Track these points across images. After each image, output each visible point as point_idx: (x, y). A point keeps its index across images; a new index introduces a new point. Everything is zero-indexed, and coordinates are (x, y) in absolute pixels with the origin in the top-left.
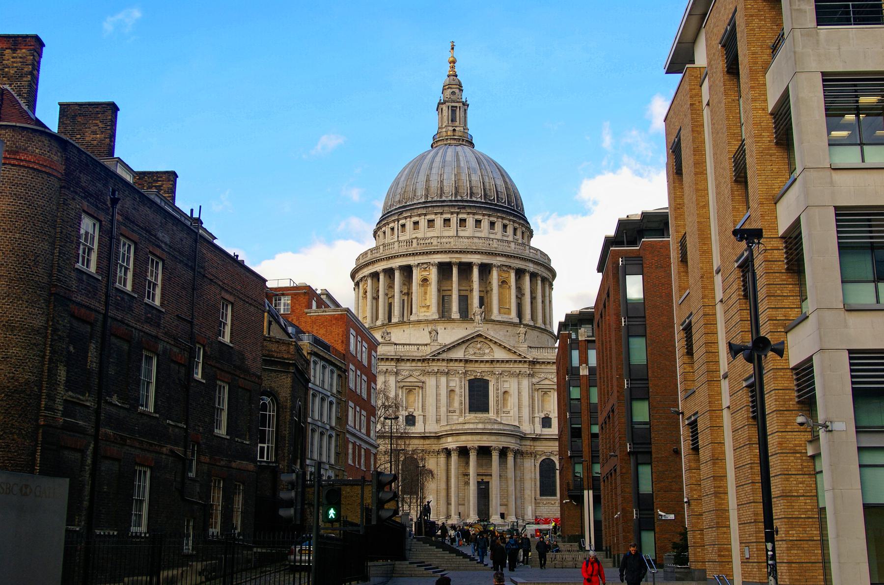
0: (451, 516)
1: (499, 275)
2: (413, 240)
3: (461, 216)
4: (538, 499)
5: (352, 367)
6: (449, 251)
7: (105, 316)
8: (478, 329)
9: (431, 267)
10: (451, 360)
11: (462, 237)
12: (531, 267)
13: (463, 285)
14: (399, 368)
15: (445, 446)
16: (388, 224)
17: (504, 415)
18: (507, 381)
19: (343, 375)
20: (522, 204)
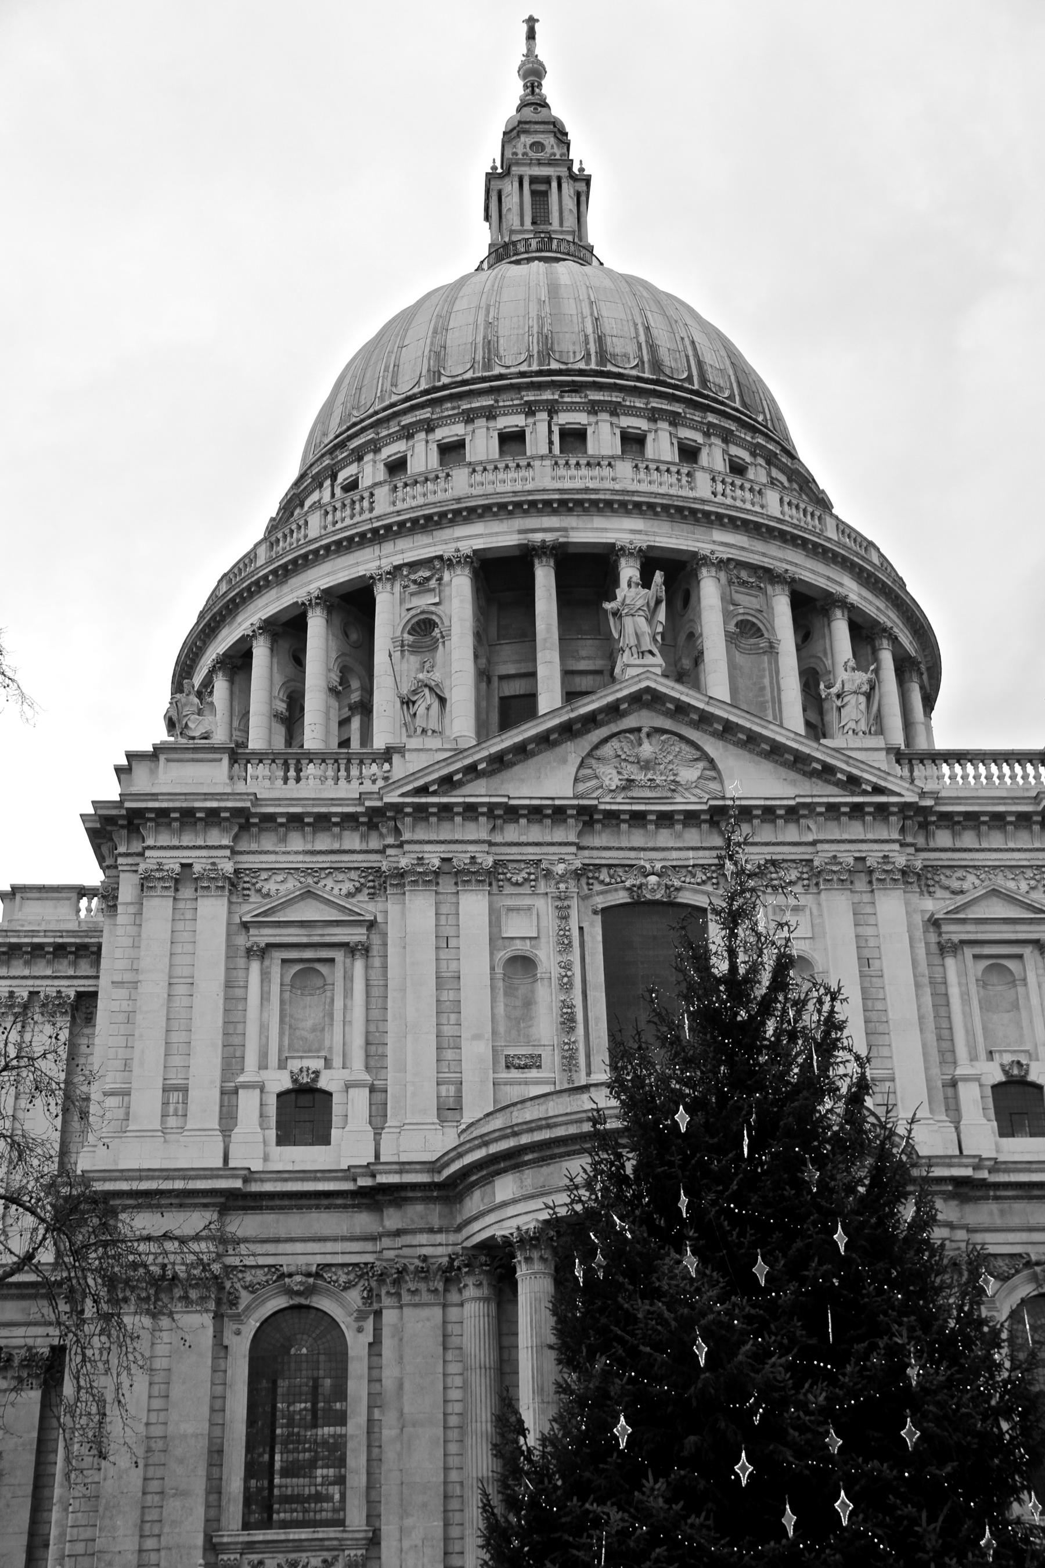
2: (376, 492)
3: (564, 418)
6: (518, 505)
9: (446, 576)
10: (511, 813)
12: (852, 590)
13: (583, 653)
14: (249, 861)
15: (481, 1231)
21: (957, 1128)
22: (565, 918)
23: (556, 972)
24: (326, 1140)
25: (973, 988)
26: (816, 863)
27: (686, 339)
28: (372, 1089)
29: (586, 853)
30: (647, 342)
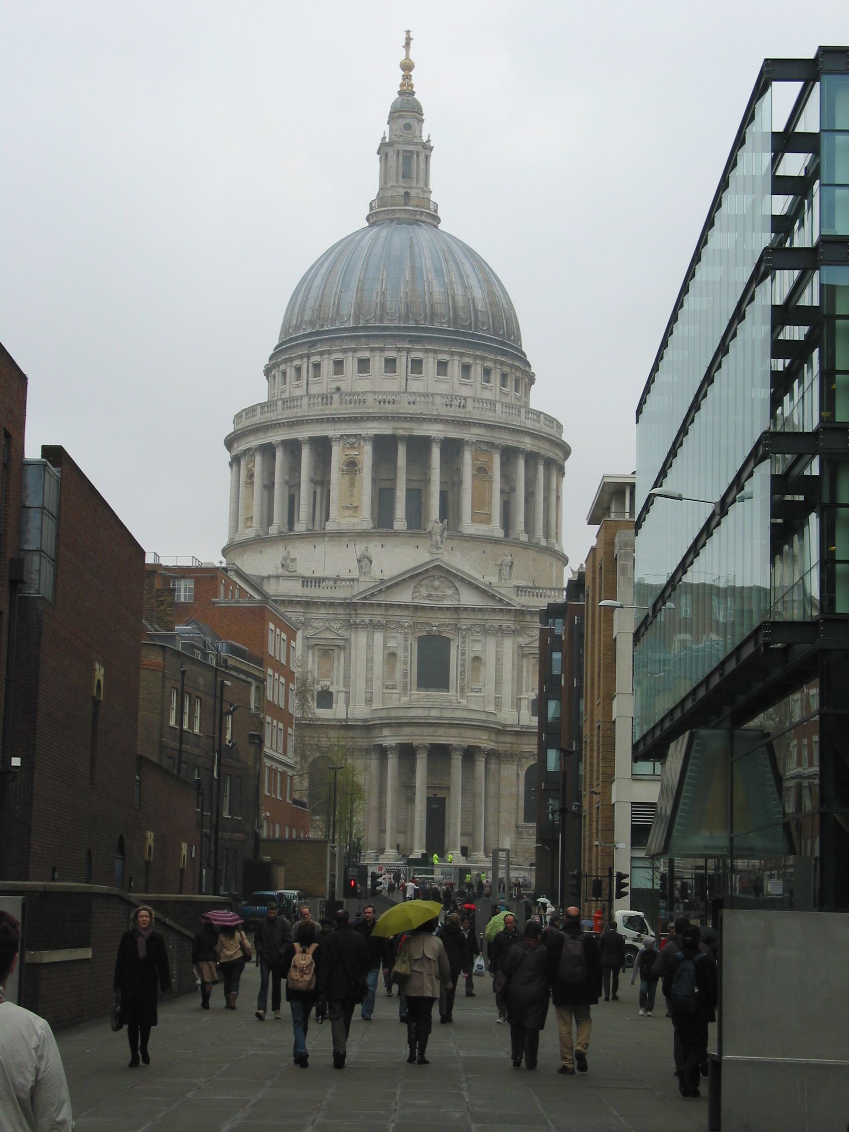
0: (384, 849)
1: (474, 459)
4: (522, 827)
5: (270, 671)
6: (393, 418)
7: (180, 751)
8: (435, 557)
9: (362, 443)
10: (392, 606)
11: (414, 393)
12: (528, 444)
14: (308, 616)
15: (378, 741)
16: (291, 360)
17: (473, 694)
18: (478, 641)
19: (261, 687)
20: (518, 328)
21: (519, 713)
22: (406, 641)
23: (402, 658)
24: (330, 707)
25: (531, 668)
26: (486, 626)
27: (470, 300)
28: (346, 693)
29: (414, 618)
30: (453, 307)
